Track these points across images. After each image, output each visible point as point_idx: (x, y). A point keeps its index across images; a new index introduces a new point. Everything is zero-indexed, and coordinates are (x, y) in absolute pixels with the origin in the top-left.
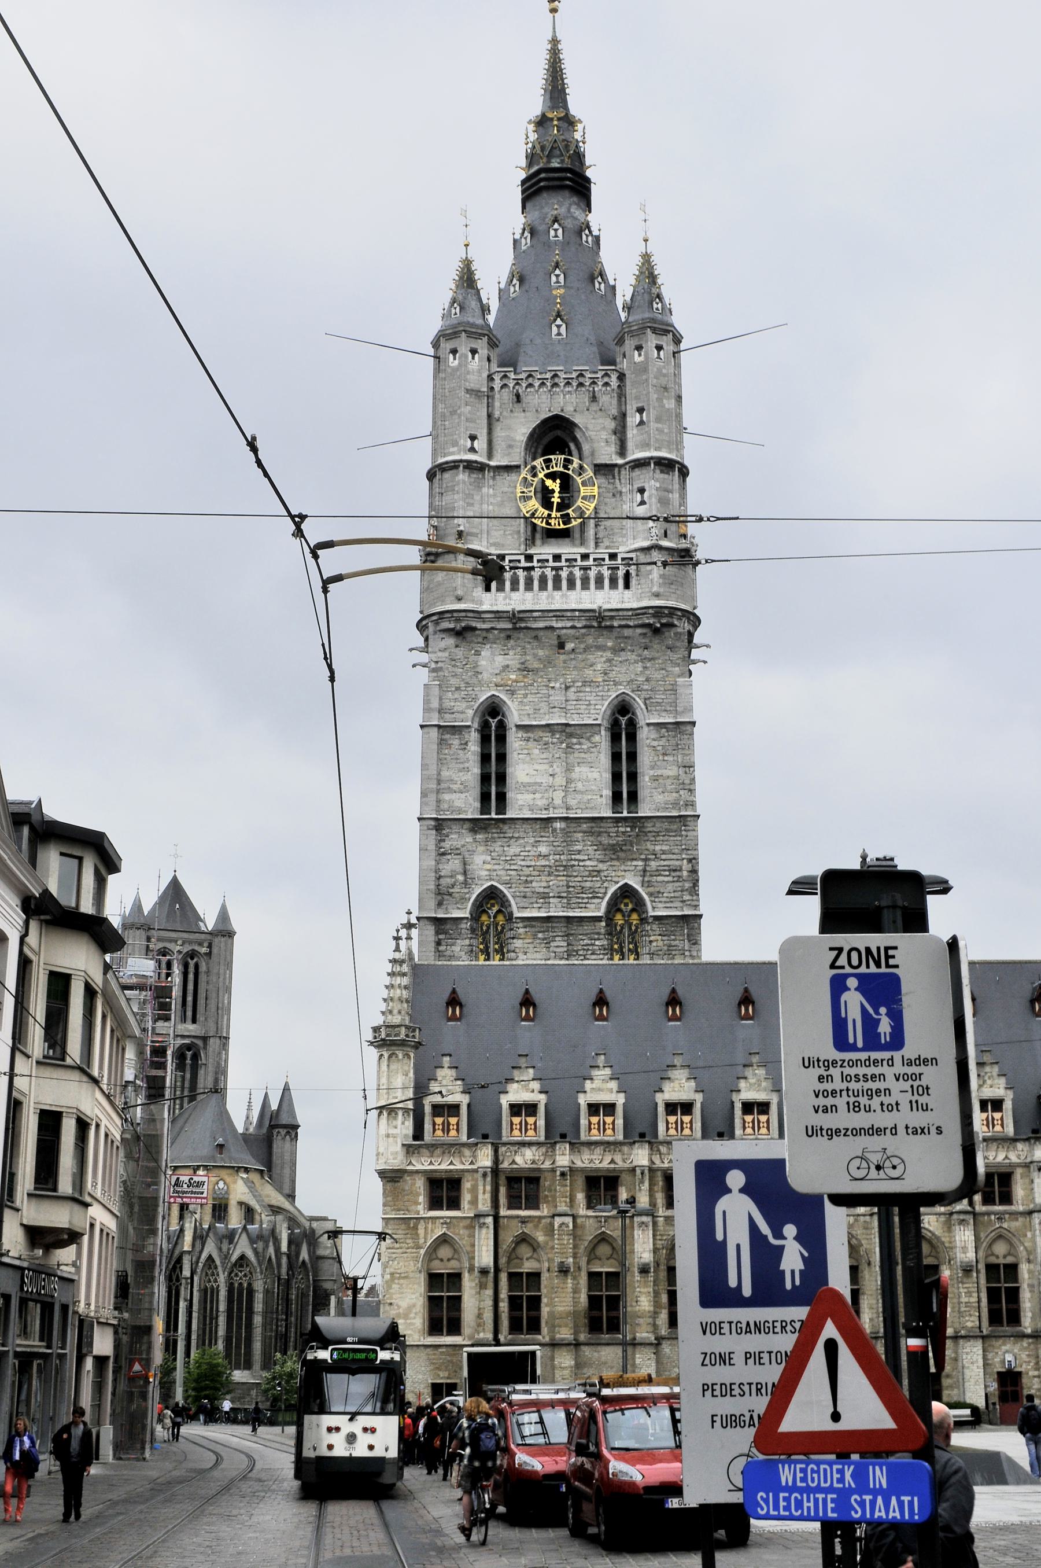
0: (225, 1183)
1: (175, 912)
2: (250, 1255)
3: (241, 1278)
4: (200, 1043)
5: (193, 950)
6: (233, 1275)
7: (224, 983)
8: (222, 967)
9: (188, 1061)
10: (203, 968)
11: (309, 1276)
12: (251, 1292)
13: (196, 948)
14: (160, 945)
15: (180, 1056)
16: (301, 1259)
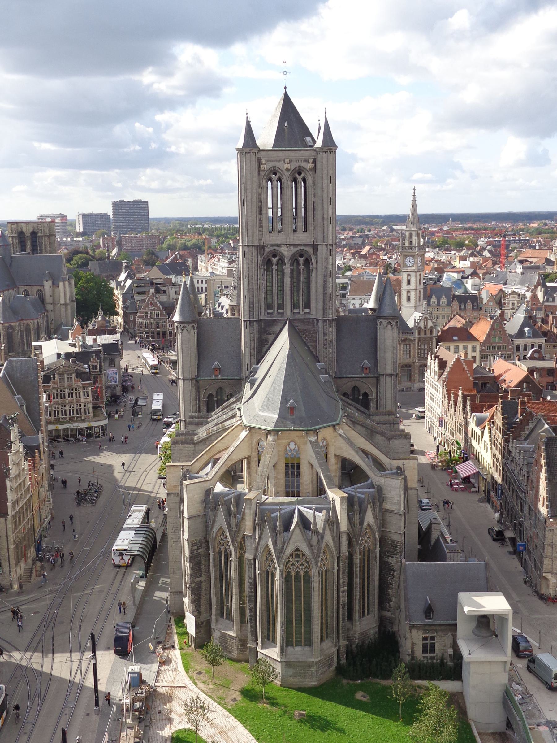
0: (295, 445)
1: (284, 130)
2: (304, 548)
3: (297, 567)
4: (310, 250)
5: (300, 166)
6: (289, 565)
7: (328, 196)
8: (325, 181)
9: (301, 267)
10: (310, 181)
11: (374, 535)
12: (308, 579)
13: (303, 164)
14: (270, 165)
15: (294, 261)
16: (365, 524)
